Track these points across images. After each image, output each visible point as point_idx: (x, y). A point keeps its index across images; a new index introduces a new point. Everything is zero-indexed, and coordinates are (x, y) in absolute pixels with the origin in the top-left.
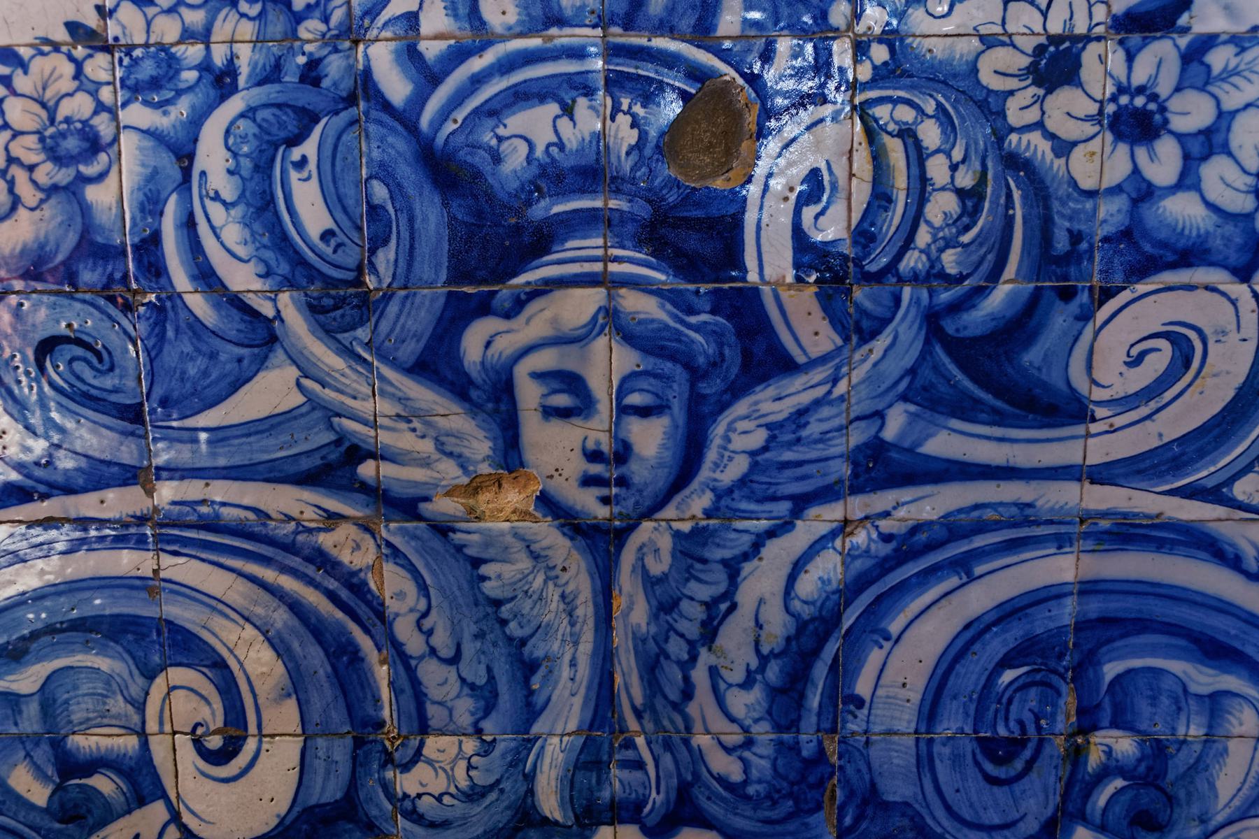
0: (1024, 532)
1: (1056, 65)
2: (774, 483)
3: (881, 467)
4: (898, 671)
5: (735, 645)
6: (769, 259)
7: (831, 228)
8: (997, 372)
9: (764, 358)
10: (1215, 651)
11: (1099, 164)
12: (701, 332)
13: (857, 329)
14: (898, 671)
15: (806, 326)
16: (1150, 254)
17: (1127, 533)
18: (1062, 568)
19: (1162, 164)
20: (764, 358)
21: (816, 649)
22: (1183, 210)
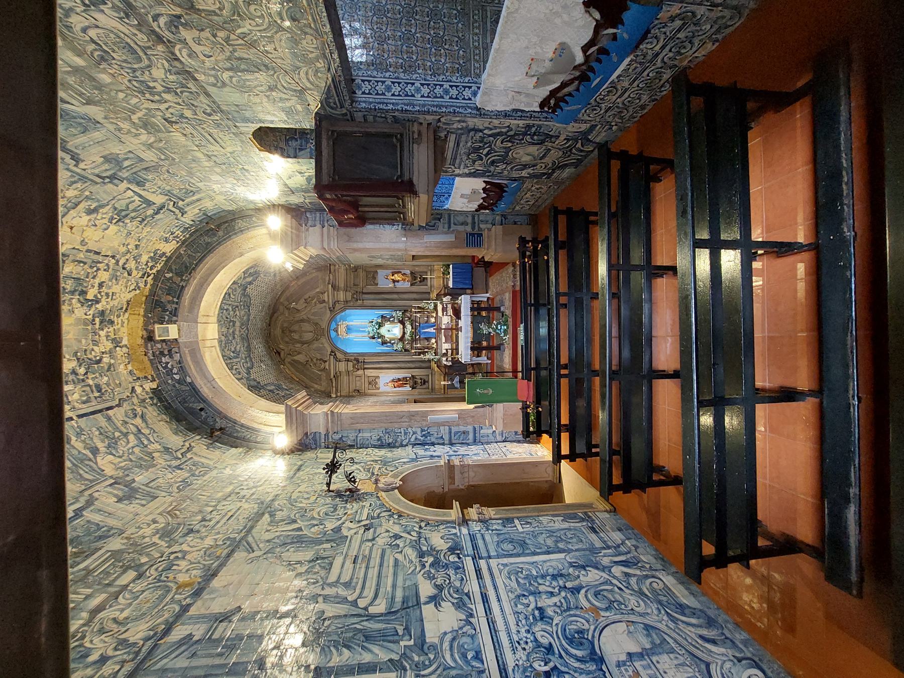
0: (561, 645)
1: (524, 649)
2: (566, 665)
3: (561, 656)
4: (579, 653)
5: (582, 666)
6: (547, 668)
7: (543, 664)
8: (549, 649)
9: (555, 668)
10: (565, 630)
11: (530, 644)
12: (556, 673)
13: (550, 660)
14: (579, 653)
15: (551, 665)
16: (536, 640)
17: (558, 638)
18: (563, 642)
19: (529, 641)
20: (555, 668)
21: (578, 659)
22: (532, 638)
